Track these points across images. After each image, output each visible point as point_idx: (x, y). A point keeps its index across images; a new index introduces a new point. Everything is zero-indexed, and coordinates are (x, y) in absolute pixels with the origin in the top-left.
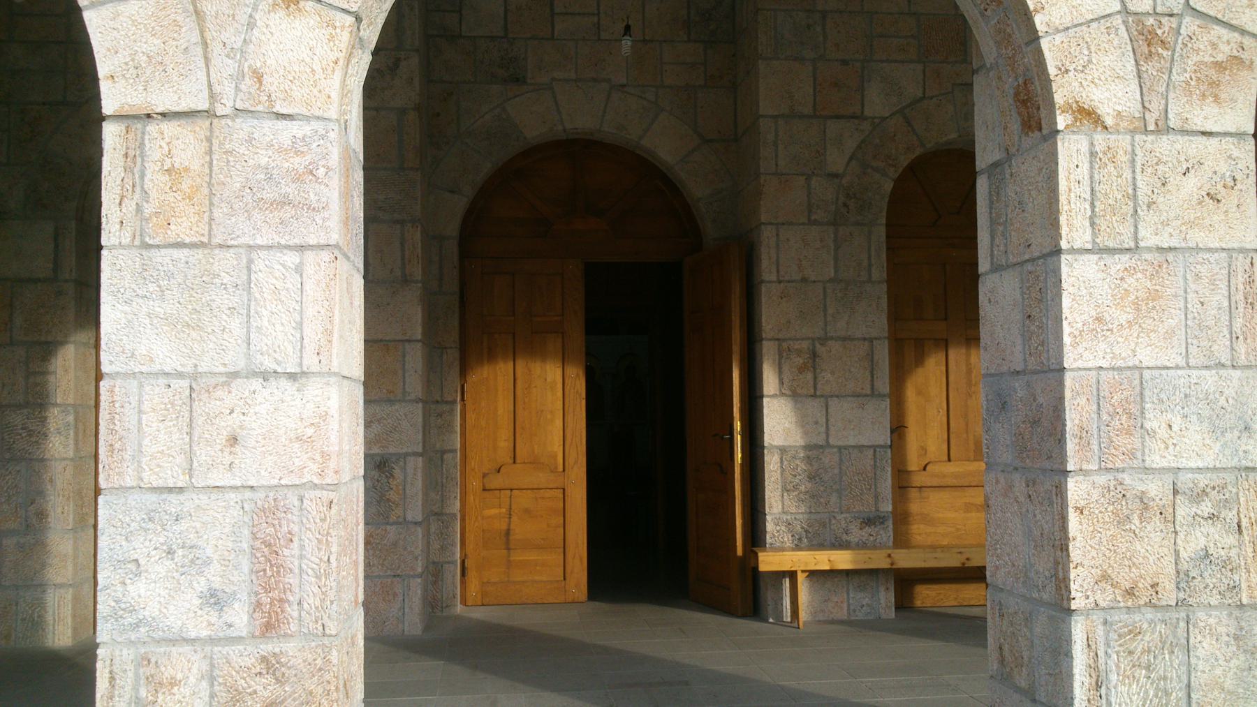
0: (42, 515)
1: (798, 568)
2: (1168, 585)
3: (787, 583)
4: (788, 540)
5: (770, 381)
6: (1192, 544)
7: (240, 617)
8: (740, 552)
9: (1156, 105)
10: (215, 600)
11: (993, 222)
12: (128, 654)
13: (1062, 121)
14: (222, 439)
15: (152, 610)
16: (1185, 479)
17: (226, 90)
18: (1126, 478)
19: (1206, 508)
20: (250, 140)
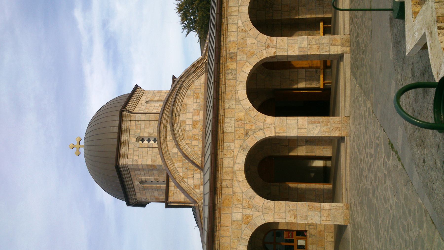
0: (313, 189)
1: (323, 82)
2: (318, 45)
3: (325, 84)
4: (319, 84)
5: (295, 87)
6: (314, 43)
7: (318, 125)
8: (321, 91)
9: (274, 46)
10: (317, 127)
11: (283, 60)
12: (321, 133)
13: (275, 55)
14: (303, 126)
15: (317, 132)
16: (308, 44)
17: (273, 126)
18: (308, 49)
19: (311, 42)
20: (277, 124)
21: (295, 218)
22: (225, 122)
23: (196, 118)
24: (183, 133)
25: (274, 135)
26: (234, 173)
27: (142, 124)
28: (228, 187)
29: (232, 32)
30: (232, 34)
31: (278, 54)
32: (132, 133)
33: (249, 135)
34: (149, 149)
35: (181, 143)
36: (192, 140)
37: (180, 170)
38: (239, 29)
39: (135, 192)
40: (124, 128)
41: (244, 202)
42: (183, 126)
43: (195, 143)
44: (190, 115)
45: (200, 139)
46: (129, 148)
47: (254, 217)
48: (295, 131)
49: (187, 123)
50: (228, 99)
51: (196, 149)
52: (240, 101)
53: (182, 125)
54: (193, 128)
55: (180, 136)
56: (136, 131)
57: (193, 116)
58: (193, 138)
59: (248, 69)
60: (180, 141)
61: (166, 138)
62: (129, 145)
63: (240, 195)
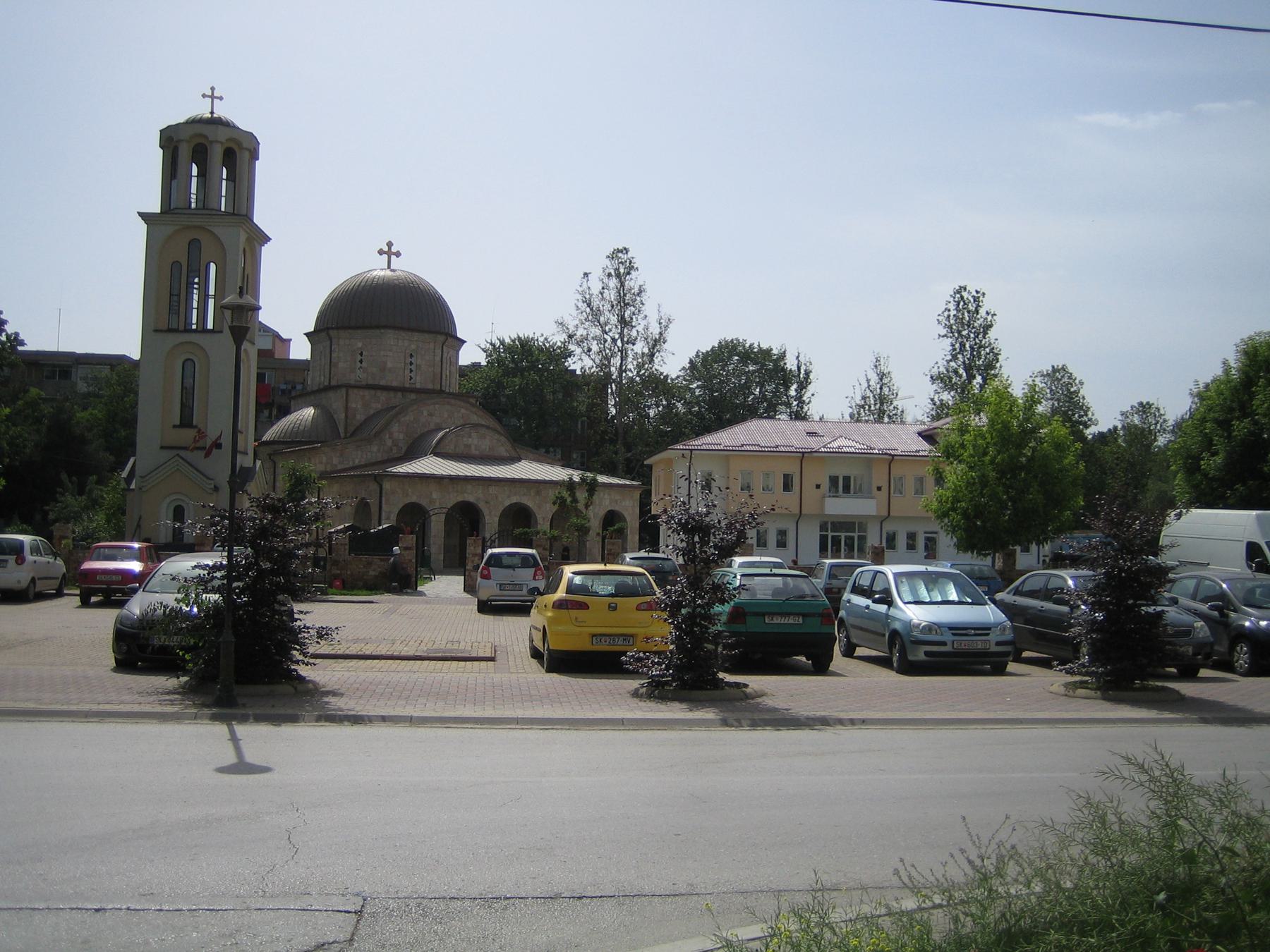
23: (473, 447)
34: (403, 364)
37: (407, 418)
40: (427, 336)
44: (475, 442)
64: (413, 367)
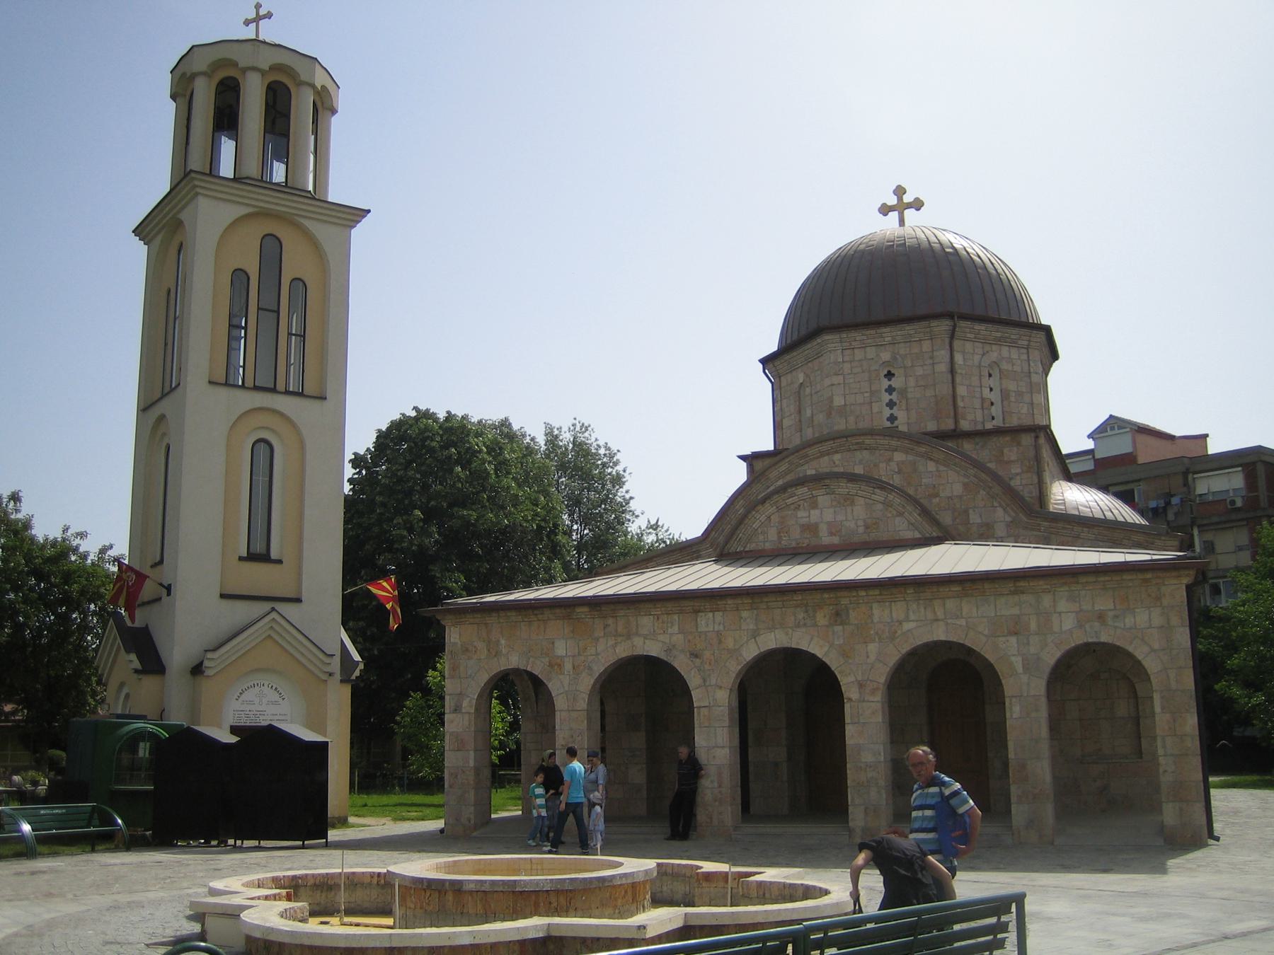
7: (716, 785)
13: (845, 701)
21: (562, 745)
22: (716, 613)
23: (823, 529)
24: (792, 507)
25: (695, 706)
26: (629, 636)
27: (925, 367)
28: (604, 628)
29: (891, 610)
30: (887, 612)
31: (847, 706)
32: (902, 349)
33: (694, 660)
35: (767, 505)
36: (779, 527)
38: (897, 624)
39: (791, 372)
40: (909, 329)
41: (582, 658)
42: (805, 504)
43: (772, 534)
44: (829, 515)
45: (780, 543)
46: (868, 349)
47: (561, 677)
48: (704, 743)
49: (812, 512)
50: (757, 615)
51: (761, 537)
52: (755, 638)
53: (807, 502)
54: (802, 526)
55: (784, 500)
56: (908, 356)
57: (829, 523)
58: (782, 528)
59: (817, 648)
60: (772, 502)
61: (837, 452)
62: (873, 348)
63: (593, 651)
64: (894, 397)
